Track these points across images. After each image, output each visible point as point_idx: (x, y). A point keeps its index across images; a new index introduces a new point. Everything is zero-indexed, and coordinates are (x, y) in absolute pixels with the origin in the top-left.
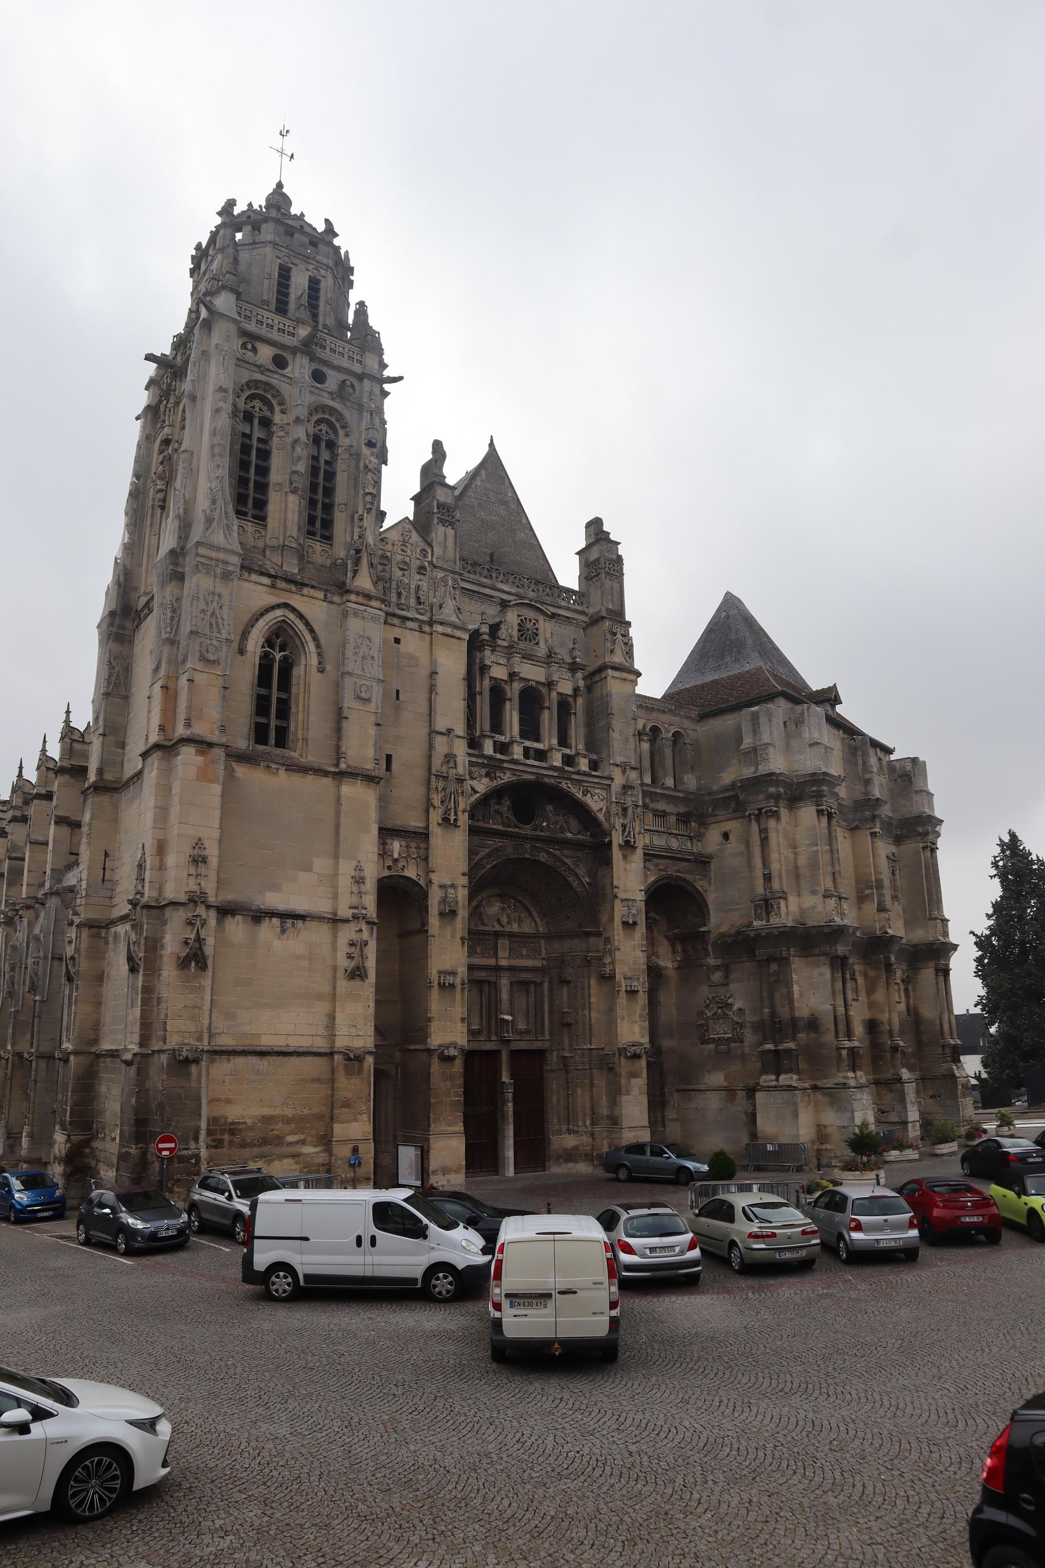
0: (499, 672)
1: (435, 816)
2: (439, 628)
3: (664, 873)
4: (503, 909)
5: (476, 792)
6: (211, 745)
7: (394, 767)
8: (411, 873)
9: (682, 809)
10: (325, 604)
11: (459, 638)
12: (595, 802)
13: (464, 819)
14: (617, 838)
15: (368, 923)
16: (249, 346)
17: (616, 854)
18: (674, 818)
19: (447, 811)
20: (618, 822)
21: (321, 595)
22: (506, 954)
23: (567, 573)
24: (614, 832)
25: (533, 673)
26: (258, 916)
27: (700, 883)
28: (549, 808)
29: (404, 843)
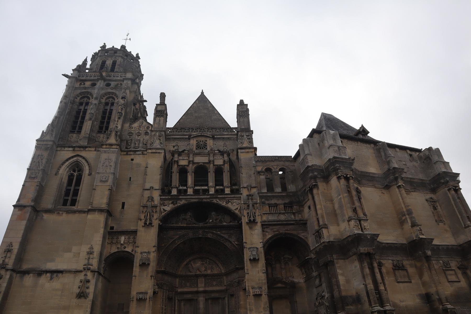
0: (183, 162)
1: (141, 223)
2: (150, 151)
3: (277, 233)
4: (203, 264)
5: (165, 211)
6: (25, 207)
7: (125, 207)
8: (129, 249)
9: (287, 201)
10: (95, 152)
11: (159, 153)
12: (233, 206)
13: (156, 223)
14: (245, 220)
15: (92, 271)
16: (83, 84)
17: (245, 228)
18: (283, 206)
19: (146, 221)
20: (245, 213)
21: (93, 149)
22: (203, 285)
23: (233, 122)
24: (243, 217)
25: (200, 160)
26: (40, 273)
27: (302, 234)
28: (213, 213)
29: (127, 237)
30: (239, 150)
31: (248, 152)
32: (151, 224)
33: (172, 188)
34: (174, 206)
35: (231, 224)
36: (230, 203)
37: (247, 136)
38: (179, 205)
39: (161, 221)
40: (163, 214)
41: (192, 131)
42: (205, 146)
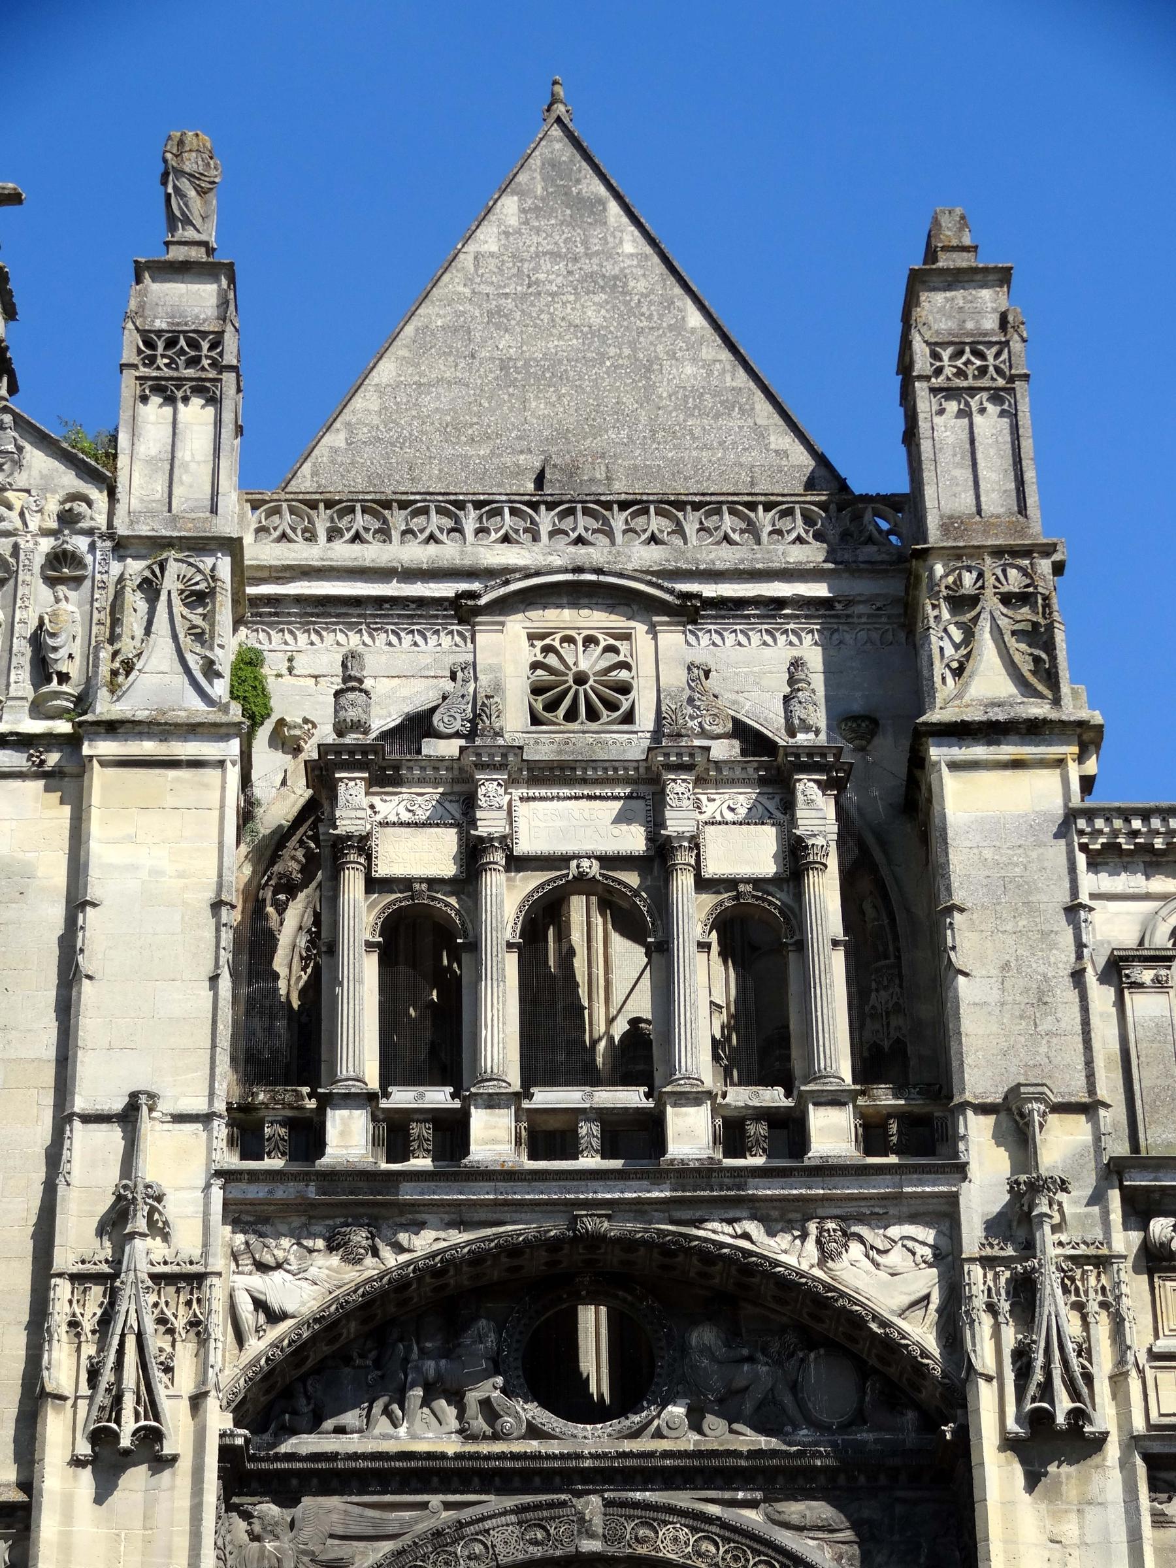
5: (274, 1317)
11: (196, 764)
12: (885, 1278)
14: (993, 1412)
20: (990, 1344)
28: (704, 1336)
30: (936, 753)
31: (1017, 764)
32: (150, 1437)
33: (326, 1102)
34: (352, 1275)
35: (865, 1436)
36: (856, 1249)
37: (1007, 599)
38: (391, 1259)
39: (241, 1412)
40: (256, 1346)
41: (481, 531)
42: (611, 699)
